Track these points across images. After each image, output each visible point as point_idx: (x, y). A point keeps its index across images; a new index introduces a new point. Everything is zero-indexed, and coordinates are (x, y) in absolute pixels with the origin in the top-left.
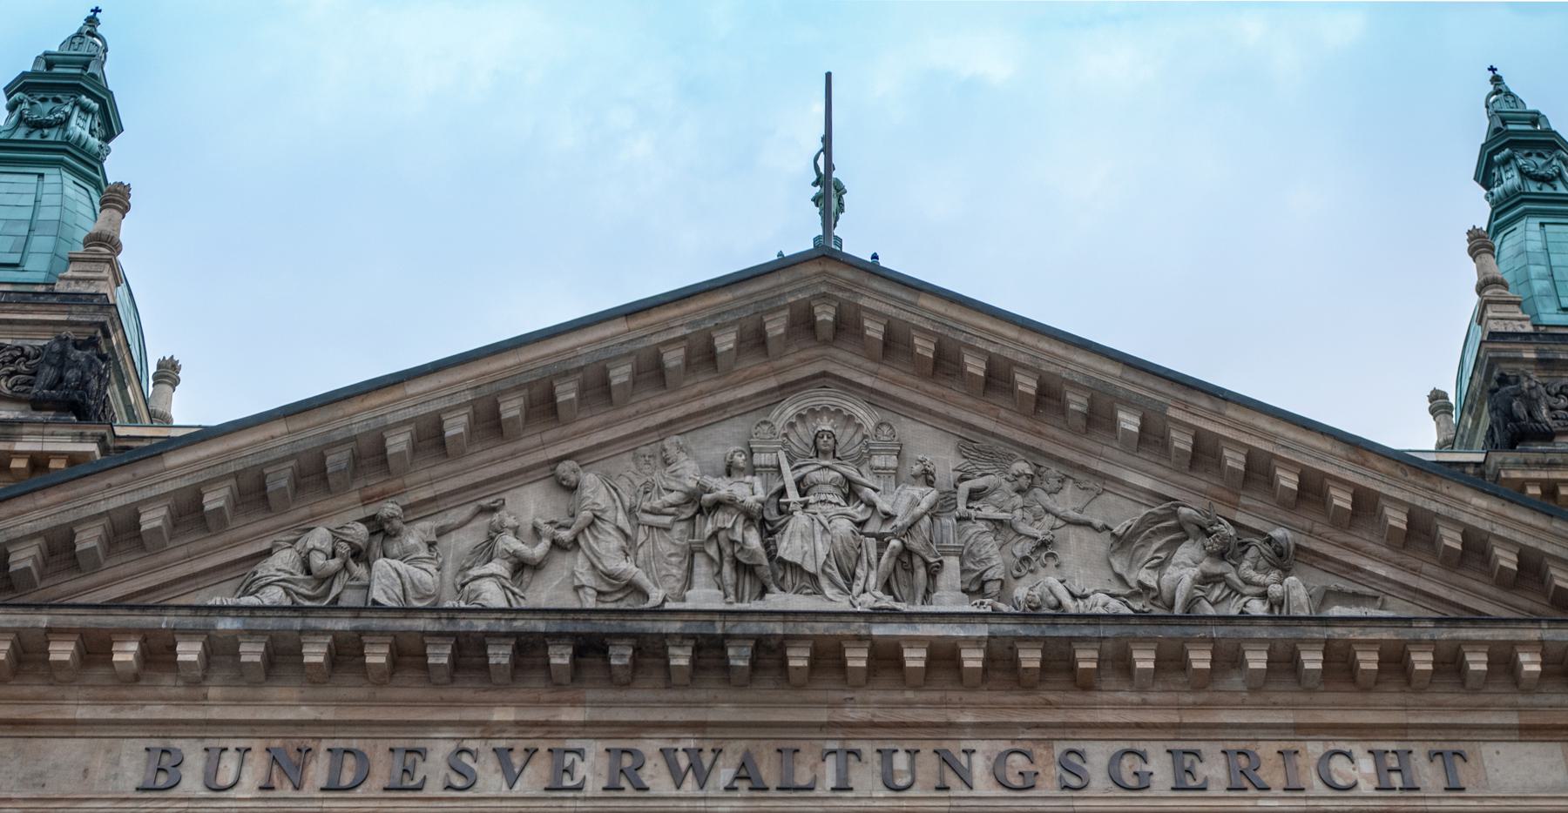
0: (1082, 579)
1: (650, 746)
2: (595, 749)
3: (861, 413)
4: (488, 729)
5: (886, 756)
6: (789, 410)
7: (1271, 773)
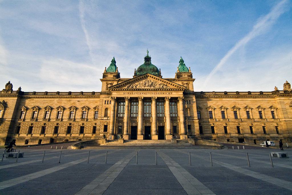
0: (157, 87)
1: (141, 93)
7: (164, 94)
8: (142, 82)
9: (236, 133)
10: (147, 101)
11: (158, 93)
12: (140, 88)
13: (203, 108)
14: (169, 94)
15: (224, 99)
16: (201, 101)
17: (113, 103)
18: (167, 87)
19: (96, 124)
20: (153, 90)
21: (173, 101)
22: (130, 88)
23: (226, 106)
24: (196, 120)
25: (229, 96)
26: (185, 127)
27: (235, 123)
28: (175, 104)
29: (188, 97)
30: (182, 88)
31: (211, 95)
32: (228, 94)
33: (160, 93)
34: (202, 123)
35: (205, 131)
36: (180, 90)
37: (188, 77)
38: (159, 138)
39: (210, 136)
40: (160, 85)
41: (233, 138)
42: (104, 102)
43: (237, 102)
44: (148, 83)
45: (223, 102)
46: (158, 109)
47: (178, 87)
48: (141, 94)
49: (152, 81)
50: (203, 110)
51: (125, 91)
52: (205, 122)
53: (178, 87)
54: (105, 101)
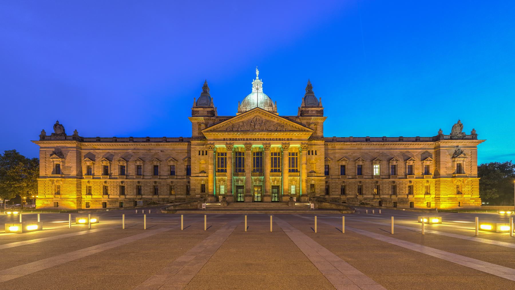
19: (189, 182)
26: (307, 186)
42: (198, 153)
54: (200, 151)
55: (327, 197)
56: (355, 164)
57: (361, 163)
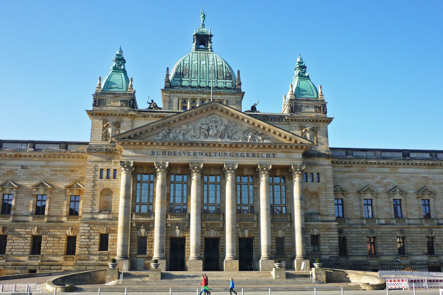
1: (197, 152)
2: (192, 152)
3: (218, 117)
4: (182, 150)
5: (219, 153)
6: (210, 117)
8: (202, 122)
9: (424, 254)
10: (212, 173)
11: (240, 153)
12: (195, 140)
13: (350, 191)
14: (268, 156)
15: (400, 170)
16: (346, 172)
17: (123, 177)
18: (263, 139)
20: (228, 146)
21: (278, 174)
22: (168, 139)
23: (405, 186)
24: (333, 221)
25: (414, 162)
27: (423, 230)
28: (283, 181)
29: (315, 165)
30: (301, 143)
31: (370, 159)
32: (412, 155)
33: (245, 155)
34: (345, 230)
35: (354, 249)
36: (297, 147)
37: (316, 112)
38: (242, 268)
39: (363, 261)
40: (244, 132)
41: (415, 264)
43: (430, 176)
44: (216, 126)
45: (399, 177)
46: (239, 193)
47: (290, 140)
48: (198, 154)
49: (226, 122)
50: (349, 195)
51: (157, 147)
52: (354, 228)
53: (290, 140)
55: (343, 260)
56: (389, 198)
57: (397, 197)
